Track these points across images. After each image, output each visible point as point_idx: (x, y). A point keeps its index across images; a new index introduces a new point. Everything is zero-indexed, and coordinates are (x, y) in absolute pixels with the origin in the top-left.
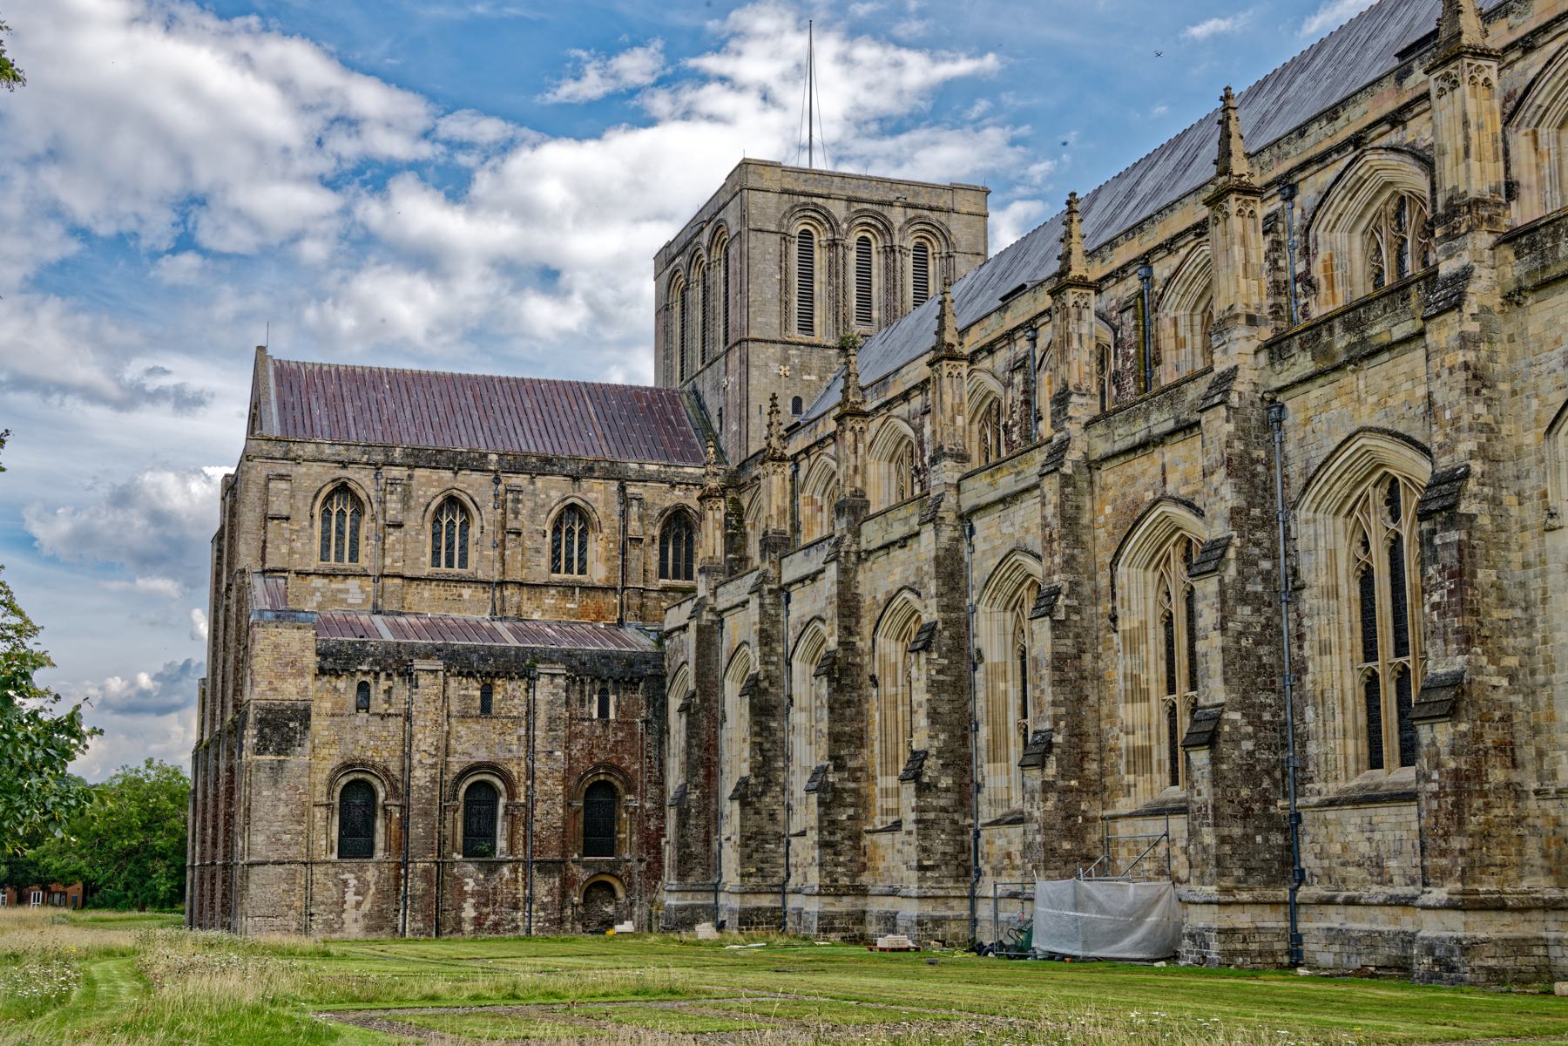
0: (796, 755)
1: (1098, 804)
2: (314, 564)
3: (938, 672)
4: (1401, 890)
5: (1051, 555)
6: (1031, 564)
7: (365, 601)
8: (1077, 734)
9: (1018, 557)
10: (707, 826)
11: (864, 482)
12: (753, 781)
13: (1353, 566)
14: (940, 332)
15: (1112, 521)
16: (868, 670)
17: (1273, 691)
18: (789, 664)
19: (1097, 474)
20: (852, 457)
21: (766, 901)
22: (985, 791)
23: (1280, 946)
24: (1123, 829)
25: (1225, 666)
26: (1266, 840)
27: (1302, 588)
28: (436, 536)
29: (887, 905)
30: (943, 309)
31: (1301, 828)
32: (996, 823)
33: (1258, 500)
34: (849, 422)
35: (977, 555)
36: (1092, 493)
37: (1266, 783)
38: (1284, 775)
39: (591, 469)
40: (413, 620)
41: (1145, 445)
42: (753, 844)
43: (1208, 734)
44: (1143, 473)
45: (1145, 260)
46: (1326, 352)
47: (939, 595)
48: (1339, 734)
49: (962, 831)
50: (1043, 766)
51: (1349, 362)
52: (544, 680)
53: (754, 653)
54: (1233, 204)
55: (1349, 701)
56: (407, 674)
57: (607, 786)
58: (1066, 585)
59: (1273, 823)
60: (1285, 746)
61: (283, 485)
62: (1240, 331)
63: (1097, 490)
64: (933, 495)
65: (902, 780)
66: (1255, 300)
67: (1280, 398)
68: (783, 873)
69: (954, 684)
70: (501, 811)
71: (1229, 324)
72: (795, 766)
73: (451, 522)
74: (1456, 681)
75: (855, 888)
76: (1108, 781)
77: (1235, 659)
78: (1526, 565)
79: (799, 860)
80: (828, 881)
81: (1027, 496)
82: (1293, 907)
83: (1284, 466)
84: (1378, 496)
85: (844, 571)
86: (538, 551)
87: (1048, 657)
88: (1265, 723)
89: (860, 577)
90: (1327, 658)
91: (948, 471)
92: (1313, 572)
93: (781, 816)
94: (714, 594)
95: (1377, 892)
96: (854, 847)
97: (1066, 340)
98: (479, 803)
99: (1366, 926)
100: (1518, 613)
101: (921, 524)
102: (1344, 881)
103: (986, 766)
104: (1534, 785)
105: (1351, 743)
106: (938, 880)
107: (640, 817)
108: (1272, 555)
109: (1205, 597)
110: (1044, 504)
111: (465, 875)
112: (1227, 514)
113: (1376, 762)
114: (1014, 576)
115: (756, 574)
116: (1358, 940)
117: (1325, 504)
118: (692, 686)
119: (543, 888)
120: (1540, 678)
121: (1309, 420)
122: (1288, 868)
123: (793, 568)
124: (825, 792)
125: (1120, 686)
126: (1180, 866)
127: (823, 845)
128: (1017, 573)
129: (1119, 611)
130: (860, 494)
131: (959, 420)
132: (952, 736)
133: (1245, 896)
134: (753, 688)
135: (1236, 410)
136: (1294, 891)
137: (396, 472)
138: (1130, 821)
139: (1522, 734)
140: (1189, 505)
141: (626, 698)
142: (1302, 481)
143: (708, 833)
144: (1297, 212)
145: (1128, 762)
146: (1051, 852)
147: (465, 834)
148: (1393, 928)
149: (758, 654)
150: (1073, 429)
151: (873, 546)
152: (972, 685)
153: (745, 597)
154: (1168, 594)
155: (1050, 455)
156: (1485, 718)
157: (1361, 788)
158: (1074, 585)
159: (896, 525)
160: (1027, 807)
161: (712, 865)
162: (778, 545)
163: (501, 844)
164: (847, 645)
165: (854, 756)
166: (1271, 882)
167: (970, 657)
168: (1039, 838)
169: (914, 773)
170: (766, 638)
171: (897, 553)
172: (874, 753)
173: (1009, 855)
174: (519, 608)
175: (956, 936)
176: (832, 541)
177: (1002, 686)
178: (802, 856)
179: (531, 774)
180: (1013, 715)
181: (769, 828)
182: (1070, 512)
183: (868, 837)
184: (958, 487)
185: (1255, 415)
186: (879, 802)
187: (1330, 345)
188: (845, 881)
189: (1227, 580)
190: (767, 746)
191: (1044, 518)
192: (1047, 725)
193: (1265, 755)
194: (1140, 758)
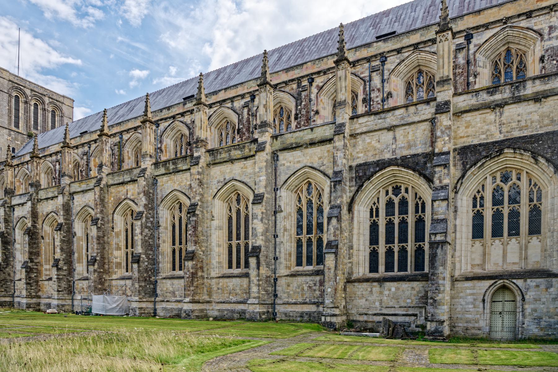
0: (17, 257)
1: (108, 276)
3: (63, 237)
4: (178, 299)
5: (97, 209)
6: (90, 210)
8: (103, 258)
14: (65, 138)
16: (41, 234)
18: (14, 229)
21: (8, 299)
22: (76, 271)
23: (152, 311)
24: (114, 283)
27: (159, 226)
29: (47, 301)
32: (79, 280)
34: (35, 159)
35: (75, 205)
37: (150, 273)
41: (122, 183)
43: (137, 260)
44: (122, 191)
46: (167, 169)
47: (64, 215)
49: (70, 281)
50: (94, 265)
51: (173, 172)
54: (148, 124)
59: (151, 283)
60: (154, 264)
64: (62, 186)
67: (157, 178)
68: (13, 291)
69: (68, 241)
72: (16, 260)
74: (193, 252)
75: (37, 296)
76: (110, 270)
77: (144, 242)
78: (207, 227)
79: (18, 288)
80: (28, 294)
82: (155, 302)
83: (157, 195)
84: (177, 206)
85: (33, 204)
87: (96, 236)
89: (38, 207)
91: (66, 181)
93: (12, 274)
95: (174, 299)
100: (205, 238)
101: (58, 194)
104: (206, 276)
105: (169, 265)
113: (174, 269)
115: (2, 201)
120: (209, 253)
121: (163, 185)
122: (154, 293)
123: (15, 201)
125: (114, 246)
126: (129, 293)
127: (27, 284)
130: (38, 182)
131: (70, 166)
132: (67, 255)
133: (144, 300)
136: (155, 299)
139: (205, 265)
140: (133, 201)
142: (161, 200)
148: (176, 307)
149: (4, 225)
150: (104, 175)
151: (43, 198)
152: (73, 242)
156: (198, 261)
157: (171, 275)
158: (103, 218)
159: (50, 193)
160: (89, 276)
165: (36, 259)
166: (150, 297)
168: (92, 284)
169: (56, 264)
171: (50, 202)
172: (42, 258)
173: (83, 288)
175: (68, 309)
176: (29, 194)
177: (81, 243)
178: (19, 286)
180: (84, 251)
181: (8, 278)
182: (102, 198)
184: (69, 185)
185: (151, 181)
186: (44, 272)
187: (169, 167)
188: (33, 294)
190: (7, 253)
191: (95, 198)
192: (95, 255)
193: (150, 266)
194: (119, 265)
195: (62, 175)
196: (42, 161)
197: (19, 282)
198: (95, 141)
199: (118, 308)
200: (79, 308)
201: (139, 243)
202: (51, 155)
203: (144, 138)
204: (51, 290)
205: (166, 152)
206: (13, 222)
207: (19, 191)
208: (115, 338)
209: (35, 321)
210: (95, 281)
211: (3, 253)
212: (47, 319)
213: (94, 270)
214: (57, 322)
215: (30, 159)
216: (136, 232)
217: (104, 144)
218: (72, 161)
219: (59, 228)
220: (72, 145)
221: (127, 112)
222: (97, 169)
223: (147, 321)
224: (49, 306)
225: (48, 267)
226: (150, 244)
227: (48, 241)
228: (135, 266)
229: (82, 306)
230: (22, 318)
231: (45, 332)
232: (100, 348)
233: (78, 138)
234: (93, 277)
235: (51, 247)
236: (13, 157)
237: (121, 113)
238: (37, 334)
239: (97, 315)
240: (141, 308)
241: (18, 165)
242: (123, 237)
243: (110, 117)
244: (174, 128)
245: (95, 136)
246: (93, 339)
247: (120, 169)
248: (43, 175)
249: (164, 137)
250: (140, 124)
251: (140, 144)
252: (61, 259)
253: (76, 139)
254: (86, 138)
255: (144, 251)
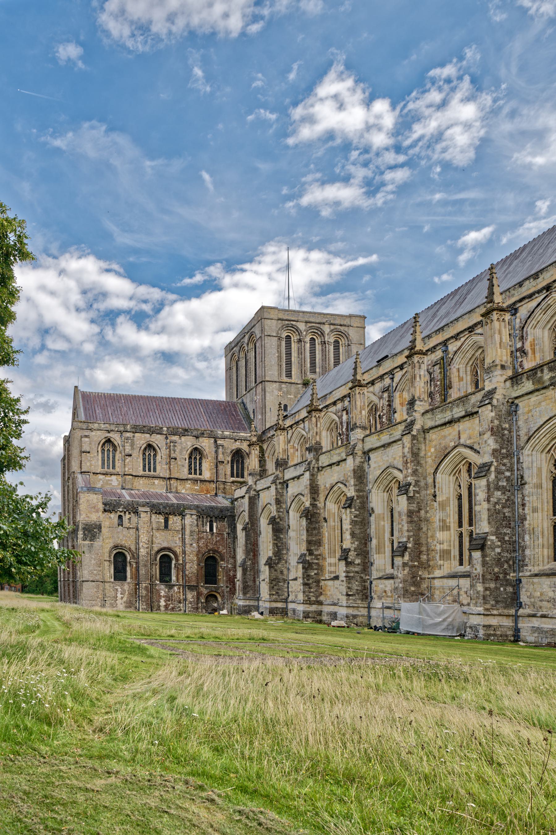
0: (291, 548)
2: (99, 470)
3: (355, 517)
6: (396, 473)
7: (119, 484)
8: (418, 543)
9: (391, 470)
10: (254, 575)
11: (320, 438)
12: (274, 558)
13: (549, 475)
14: (355, 374)
15: (435, 455)
16: (323, 516)
17: (510, 527)
18: (288, 512)
19: (427, 435)
20: (315, 428)
21: (280, 605)
22: (375, 566)
23: (510, 633)
25: (489, 516)
26: (505, 590)
28: (144, 459)
30: (356, 365)
31: (521, 585)
32: (380, 578)
33: (505, 446)
34: (314, 414)
35: (372, 468)
36: (425, 443)
37: (506, 566)
38: (514, 563)
39: (203, 434)
40: (137, 492)
42: (274, 583)
44: (449, 434)
45: (445, 343)
46: (540, 380)
47: (355, 485)
48: (540, 547)
49: (365, 581)
50: (403, 556)
51: (551, 385)
52: (188, 516)
53: (273, 508)
54: (495, 315)
55: (546, 532)
56: (136, 512)
57: (213, 558)
58: (414, 482)
59: (508, 583)
60: (514, 551)
61: (87, 439)
62: (498, 372)
63: (427, 442)
64: (352, 444)
65: (339, 560)
66: (505, 358)
67: (516, 401)
68: (286, 594)
69: (361, 522)
70: (173, 566)
71: (492, 369)
72: (291, 553)
73: (150, 454)
75: (318, 602)
76: (431, 563)
77: (493, 514)
80: (306, 598)
81: (394, 444)
82: (516, 618)
83: (517, 431)
85: (312, 475)
86: (183, 466)
87: (406, 511)
88: (506, 541)
89: (319, 478)
90: (535, 515)
91: (358, 434)
92: (530, 477)
93: (285, 572)
94: (256, 484)
96: (317, 586)
97: (414, 377)
98: (165, 562)
99: (551, 627)
101: (347, 456)
102: (541, 607)
103: (375, 556)
105: (546, 551)
106: (354, 600)
107: (227, 570)
108: (511, 470)
109: (480, 487)
110: (403, 448)
111: (160, 589)
112: (491, 452)
114: (388, 478)
115: (273, 476)
116: (547, 632)
117: (537, 447)
118: (247, 520)
119: (190, 596)
121: (530, 411)
123: (289, 474)
124: (305, 563)
125: (437, 524)
126: (465, 600)
127: (305, 584)
128: (389, 477)
129: (437, 493)
130: (318, 443)
131: (363, 412)
132: (361, 543)
133: (495, 612)
134: (273, 521)
135: (496, 407)
136: (517, 611)
137: (128, 435)
138: (441, 580)
140: (471, 448)
141: (220, 524)
142: (526, 438)
143: (254, 578)
144: (518, 321)
145: (440, 556)
146: (406, 591)
147: (160, 574)
150: (417, 415)
152: (369, 523)
153: (269, 485)
154: (460, 486)
155: (406, 427)
158: (417, 482)
160: (395, 573)
161: (256, 590)
162: (281, 464)
163: (174, 578)
164: (313, 505)
165: (317, 550)
166: (506, 607)
167: (368, 511)
168: (401, 585)
170: (278, 502)
171: (335, 468)
172: (325, 549)
173: (385, 592)
174: (177, 488)
175: (362, 622)
176: (307, 463)
177: (382, 523)
179: (184, 552)
181: (280, 577)
182: (415, 451)
183: (323, 582)
184: (363, 440)
185: (504, 409)
186: (327, 568)
187: (541, 378)
188: (313, 599)
189: (490, 480)
190: (279, 545)
191: (403, 453)
192: (405, 540)
193: (506, 554)
194: (445, 554)
195: (351, 427)
196: (323, 414)
197: (295, 582)
198: (401, 367)
199: (446, 624)
200: (380, 621)
201: (485, 516)
202: (334, 403)
203: (489, 340)
204: (338, 593)
205: (534, 352)
206: (286, 503)
207: (293, 459)
208: (443, 673)
209: (315, 636)
210: (405, 581)
211: (274, 543)
212: (332, 635)
213: (403, 563)
214: (347, 640)
215: (306, 415)
216: (478, 498)
217: (417, 368)
218: (366, 404)
219: (349, 503)
220: (365, 382)
221: (453, 307)
222: (405, 408)
223: (501, 650)
224: (334, 616)
225: (332, 560)
226: (505, 517)
227: (332, 524)
228: (477, 555)
229: (384, 618)
230: (299, 631)
231: (330, 652)
232: (418, 685)
233: (374, 369)
234: (401, 574)
235: (338, 532)
236: (286, 417)
237: (443, 311)
238: (320, 655)
239: (408, 633)
240: (488, 627)
241: (291, 426)
242: (453, 508)
243: (425, 323)
244: (549, 306)
245: (401, 359)
246: (406, 671)
247: (445, 400)
248: (324, 433)
249: (529, 329)
250: (481, 318)
251: (480, 351)
252: (352, 549)
253: (371, 372)
254: (387, 366)
255: (494, 530)
